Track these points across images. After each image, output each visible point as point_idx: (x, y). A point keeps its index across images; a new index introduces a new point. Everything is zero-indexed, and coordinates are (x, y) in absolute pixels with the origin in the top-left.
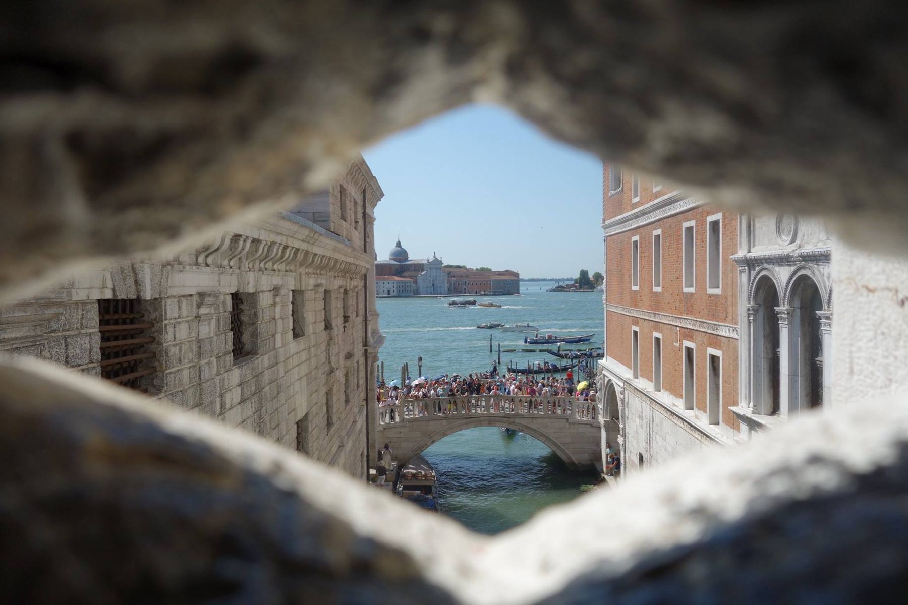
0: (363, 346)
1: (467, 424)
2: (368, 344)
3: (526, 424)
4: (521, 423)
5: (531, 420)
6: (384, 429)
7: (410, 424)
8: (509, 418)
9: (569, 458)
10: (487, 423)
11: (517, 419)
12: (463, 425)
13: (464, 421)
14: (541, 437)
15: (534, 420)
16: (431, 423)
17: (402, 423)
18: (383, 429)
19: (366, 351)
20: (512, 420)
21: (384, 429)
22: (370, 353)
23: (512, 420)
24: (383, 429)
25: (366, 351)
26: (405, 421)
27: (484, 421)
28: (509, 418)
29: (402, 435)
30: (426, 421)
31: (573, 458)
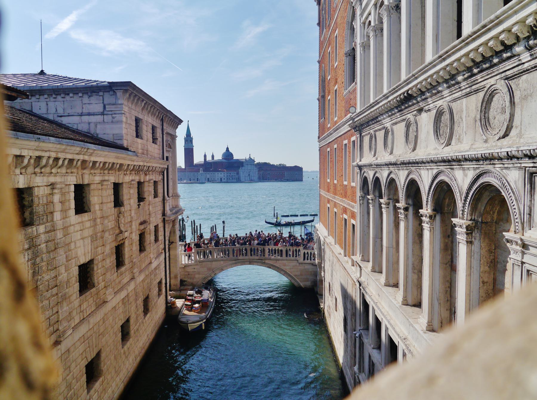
1: (236, 263)
5: (275, 261)
7: (201, 263)
8: (262, 260)
9: (299, 284)
13: (234, 262)
15: (278, 261)
16: (214, 263)
19: (164, 219)
20: (264, 261)
22: (167, 220)
23: (264, 261)
25: (164, 219)
27: (246, 261)
28: (262, 260)
29: (196, 270)
30: (210, 261)
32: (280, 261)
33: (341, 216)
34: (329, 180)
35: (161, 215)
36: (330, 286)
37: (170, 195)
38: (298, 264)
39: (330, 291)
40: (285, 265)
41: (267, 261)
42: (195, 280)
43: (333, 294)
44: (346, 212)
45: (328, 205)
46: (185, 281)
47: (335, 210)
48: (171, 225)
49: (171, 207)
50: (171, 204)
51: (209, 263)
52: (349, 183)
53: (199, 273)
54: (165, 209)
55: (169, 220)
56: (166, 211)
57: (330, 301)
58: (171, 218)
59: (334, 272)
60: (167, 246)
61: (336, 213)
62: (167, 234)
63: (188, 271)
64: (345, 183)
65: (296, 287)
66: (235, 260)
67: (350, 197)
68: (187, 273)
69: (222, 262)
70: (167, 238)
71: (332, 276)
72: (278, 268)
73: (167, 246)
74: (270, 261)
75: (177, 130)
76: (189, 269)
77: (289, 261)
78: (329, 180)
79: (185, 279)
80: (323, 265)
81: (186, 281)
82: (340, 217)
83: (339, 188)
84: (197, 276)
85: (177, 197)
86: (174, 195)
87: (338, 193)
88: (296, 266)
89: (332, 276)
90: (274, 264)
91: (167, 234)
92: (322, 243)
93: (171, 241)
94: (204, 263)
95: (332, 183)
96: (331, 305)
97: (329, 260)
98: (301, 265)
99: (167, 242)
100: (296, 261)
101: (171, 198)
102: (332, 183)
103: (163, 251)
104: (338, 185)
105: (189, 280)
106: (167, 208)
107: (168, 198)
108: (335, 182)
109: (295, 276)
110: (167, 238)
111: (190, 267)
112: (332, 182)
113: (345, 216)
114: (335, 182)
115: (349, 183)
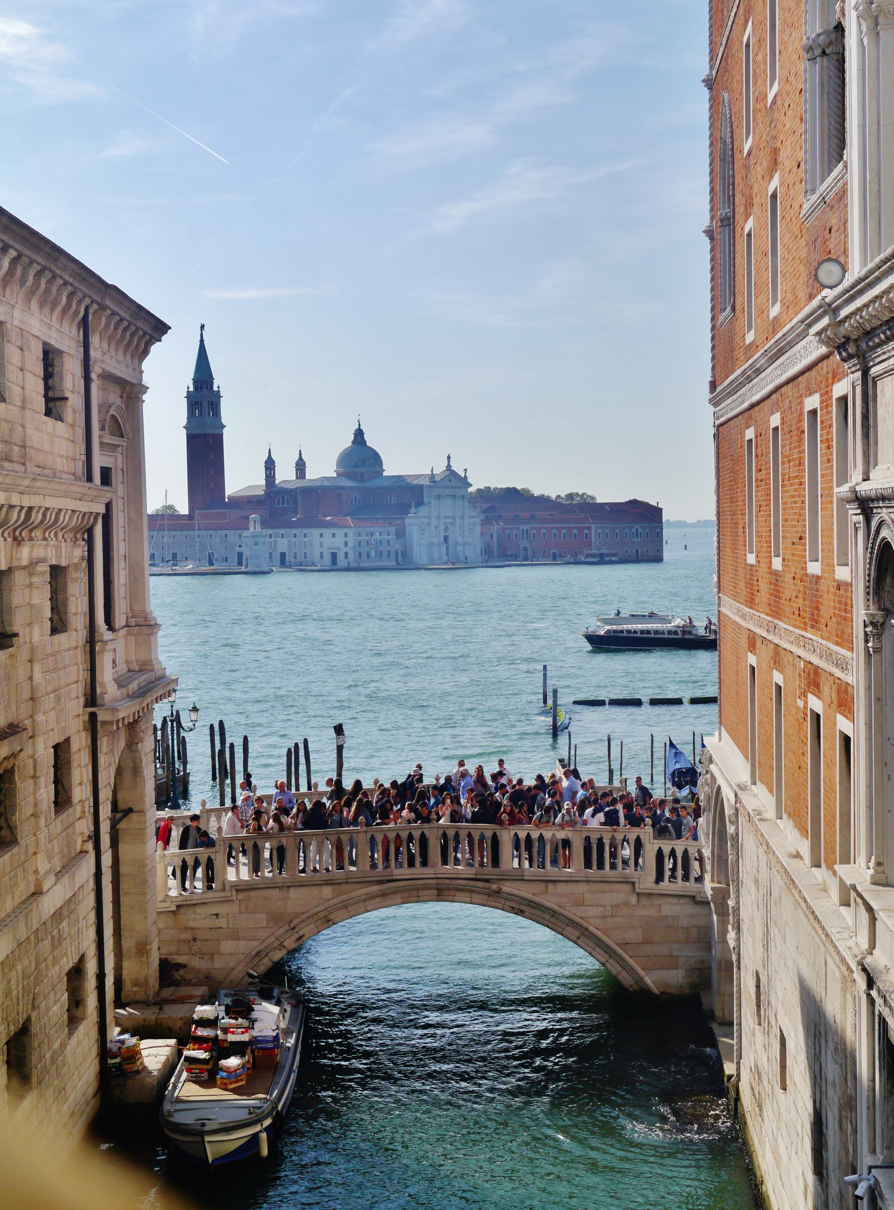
0: (86, 706)
1: (383, 895)
2: (99, 701)
3: (529, 896)
4: (516, 892)
5: (542, 886)
6: (178, 907)
7: (241, 896)
8: (487, 881)
9: (639, 980)
10: (435, 892)
11: (508, 884)
12: (373, 898)
13: (375, 888)
14: (569, 928)
15: (551, 886)
16: (294, 893)
17: (222, 894)
18: (174, 908)
19: (93, 717)
20: (494, 887)
21: (178, 907)
22: (104, 723)
23: (494, 887)
24: (174, 908)
25: (93, 717)
26: (227, 888)
27: (425, 888)
28: (487, 881)
29: (222, 922)
30: (281, 888)
31: (647, 980)
32: (561, 888)
33: (801, 703)
34: (751, 559)
35: (82, 700)
36: (758, 987)
37: (119, 620)
38: (633, 899)
39: (758, 1006)
40: (580, 903)
41: (507, 888)
42: (218, 963)
43: (773, 1022)
44: (817, 686)
45: (752, 660)
46: (180, 966)
47: (778, 677)
48: (122, 743)
49: (122, 668)
50: (121, 657)
51: (275, 893)
52: (828, 567)
53: (235, 936)
54: (99, 678)
55: (111, 723)
56: (103, 685)
57: (759, 1047)
58: (121, 715)
59: (774, 931)
60: (105, 827)
61: (779, 688)
62: (107, 777)
63: (192, 924)
64: (814, 568)
65: (627, 990)
66: (381, 882)
67: (833, 624)
68: (186, 936)
69: (327, 891)
70: (105, 795)
71: (766, 947)
72: (554, 913)
73: (105, 827)
74: (519, 885)
75: (146, 364)
76: (198, 919)
77: (599, 886)
78: (751, 559)
79: (180, 959)
80: (731, 903)
81: (184, 966)
82: (798, 708)
83: (789, 589)
84: (227, 946)
85: (146, 630)
86: (133, 622)
87: (788, 610)
88: (627, 904)
89: (766, 947)
90: (537, 899)
91: (107, 777)
92: (728, 812)
93: (122, 805)
94: (253, 894)
95: (763, 571)
96: (763, 1063)
97: (757, 881)
98: (644, 901)
99: (105, 811)
100: (627, 888)
101: (123, 632)
102: (763, 571)
103: (90, 846)
104: (788, 577)
105: (197, 963)
106: (106, 675)
107: (108, 635)
108: (777, 564)
109: (623, 945)
110: (105, 795)
111: (201, 910)
112: (764, 565)
113: (815, 704)
114: (777, 564)
115: (828, 567)
